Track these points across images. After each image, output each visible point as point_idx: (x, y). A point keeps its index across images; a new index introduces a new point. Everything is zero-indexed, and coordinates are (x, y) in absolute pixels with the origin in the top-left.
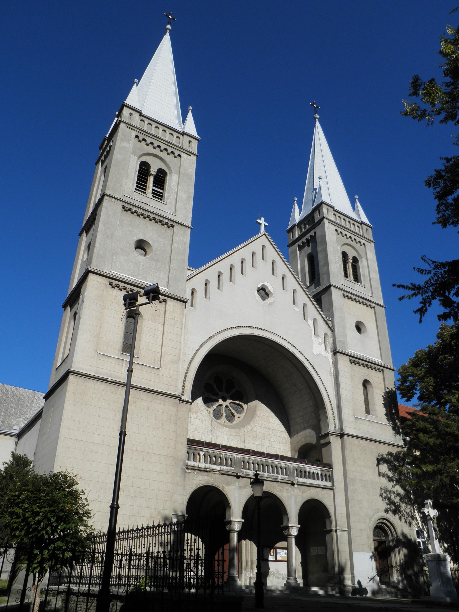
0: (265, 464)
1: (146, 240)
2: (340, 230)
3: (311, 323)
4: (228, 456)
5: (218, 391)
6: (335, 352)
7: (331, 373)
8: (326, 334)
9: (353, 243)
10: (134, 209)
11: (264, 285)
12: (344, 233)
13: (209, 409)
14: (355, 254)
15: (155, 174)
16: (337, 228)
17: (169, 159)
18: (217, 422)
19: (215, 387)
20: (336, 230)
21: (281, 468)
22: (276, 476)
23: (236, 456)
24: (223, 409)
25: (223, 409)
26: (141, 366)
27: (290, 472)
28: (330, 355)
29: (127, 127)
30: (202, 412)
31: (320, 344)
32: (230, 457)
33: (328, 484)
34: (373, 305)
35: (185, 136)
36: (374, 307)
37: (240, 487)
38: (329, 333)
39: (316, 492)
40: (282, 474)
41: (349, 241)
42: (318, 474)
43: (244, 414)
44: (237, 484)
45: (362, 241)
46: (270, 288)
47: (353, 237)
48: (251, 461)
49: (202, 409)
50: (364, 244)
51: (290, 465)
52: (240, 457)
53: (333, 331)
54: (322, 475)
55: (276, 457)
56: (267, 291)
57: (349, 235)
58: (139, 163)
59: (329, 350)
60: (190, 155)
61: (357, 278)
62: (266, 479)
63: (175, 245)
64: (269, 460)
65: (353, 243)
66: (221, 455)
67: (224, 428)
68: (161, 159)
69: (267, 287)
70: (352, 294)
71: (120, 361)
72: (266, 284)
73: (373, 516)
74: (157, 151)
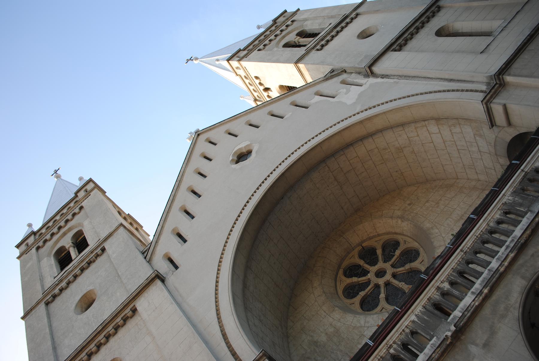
0: (469, 257)
1: (85, 292)
4: (402, 337)
5: (364, 278)
6: (369, 71)
7: (395, 82)
8: (343, 82)
10: (57, 291)
11: (235, 152)
13: (379, 308)
15: (71, 244)
18: (376, 313)
19: (355, 279)
20: (259, 50)
21: (499, 222)
22: (513, 240)
23: (413, 318)
24: (395, 282)
25: (395, 282)
27: (521, 205)
28: (372, 80)
30: (367, 325)
31: (348, 91)
32: (407, 331)
34: (353, 15)
37: (486, 345)
38: (344, 76)
40: (516, 223)
43: (421, 251)
44: (473, 349)
48: (446, 286)
49: (362, 322)
51: (504, 200)
52: (420, 308)
53: (345, 71)
55: (470, 224)
56: (244, 151)
59: (360, 80)
62: (502, 269)
64: (469, 242)
66: (392, 351)
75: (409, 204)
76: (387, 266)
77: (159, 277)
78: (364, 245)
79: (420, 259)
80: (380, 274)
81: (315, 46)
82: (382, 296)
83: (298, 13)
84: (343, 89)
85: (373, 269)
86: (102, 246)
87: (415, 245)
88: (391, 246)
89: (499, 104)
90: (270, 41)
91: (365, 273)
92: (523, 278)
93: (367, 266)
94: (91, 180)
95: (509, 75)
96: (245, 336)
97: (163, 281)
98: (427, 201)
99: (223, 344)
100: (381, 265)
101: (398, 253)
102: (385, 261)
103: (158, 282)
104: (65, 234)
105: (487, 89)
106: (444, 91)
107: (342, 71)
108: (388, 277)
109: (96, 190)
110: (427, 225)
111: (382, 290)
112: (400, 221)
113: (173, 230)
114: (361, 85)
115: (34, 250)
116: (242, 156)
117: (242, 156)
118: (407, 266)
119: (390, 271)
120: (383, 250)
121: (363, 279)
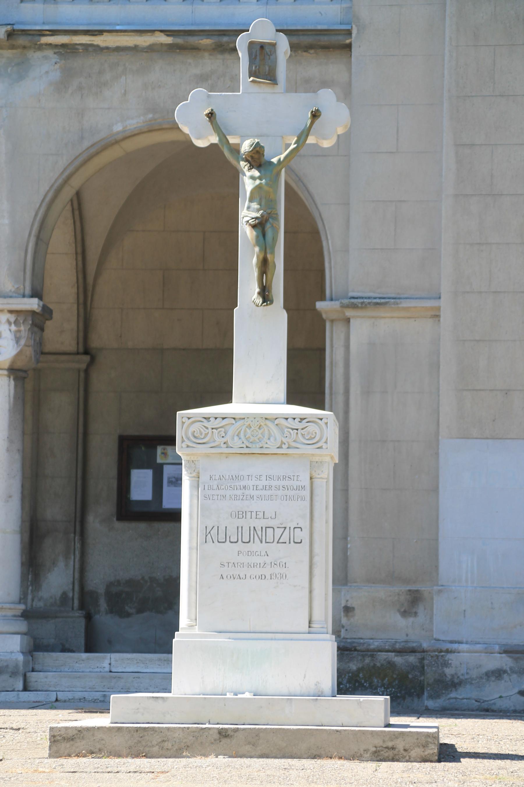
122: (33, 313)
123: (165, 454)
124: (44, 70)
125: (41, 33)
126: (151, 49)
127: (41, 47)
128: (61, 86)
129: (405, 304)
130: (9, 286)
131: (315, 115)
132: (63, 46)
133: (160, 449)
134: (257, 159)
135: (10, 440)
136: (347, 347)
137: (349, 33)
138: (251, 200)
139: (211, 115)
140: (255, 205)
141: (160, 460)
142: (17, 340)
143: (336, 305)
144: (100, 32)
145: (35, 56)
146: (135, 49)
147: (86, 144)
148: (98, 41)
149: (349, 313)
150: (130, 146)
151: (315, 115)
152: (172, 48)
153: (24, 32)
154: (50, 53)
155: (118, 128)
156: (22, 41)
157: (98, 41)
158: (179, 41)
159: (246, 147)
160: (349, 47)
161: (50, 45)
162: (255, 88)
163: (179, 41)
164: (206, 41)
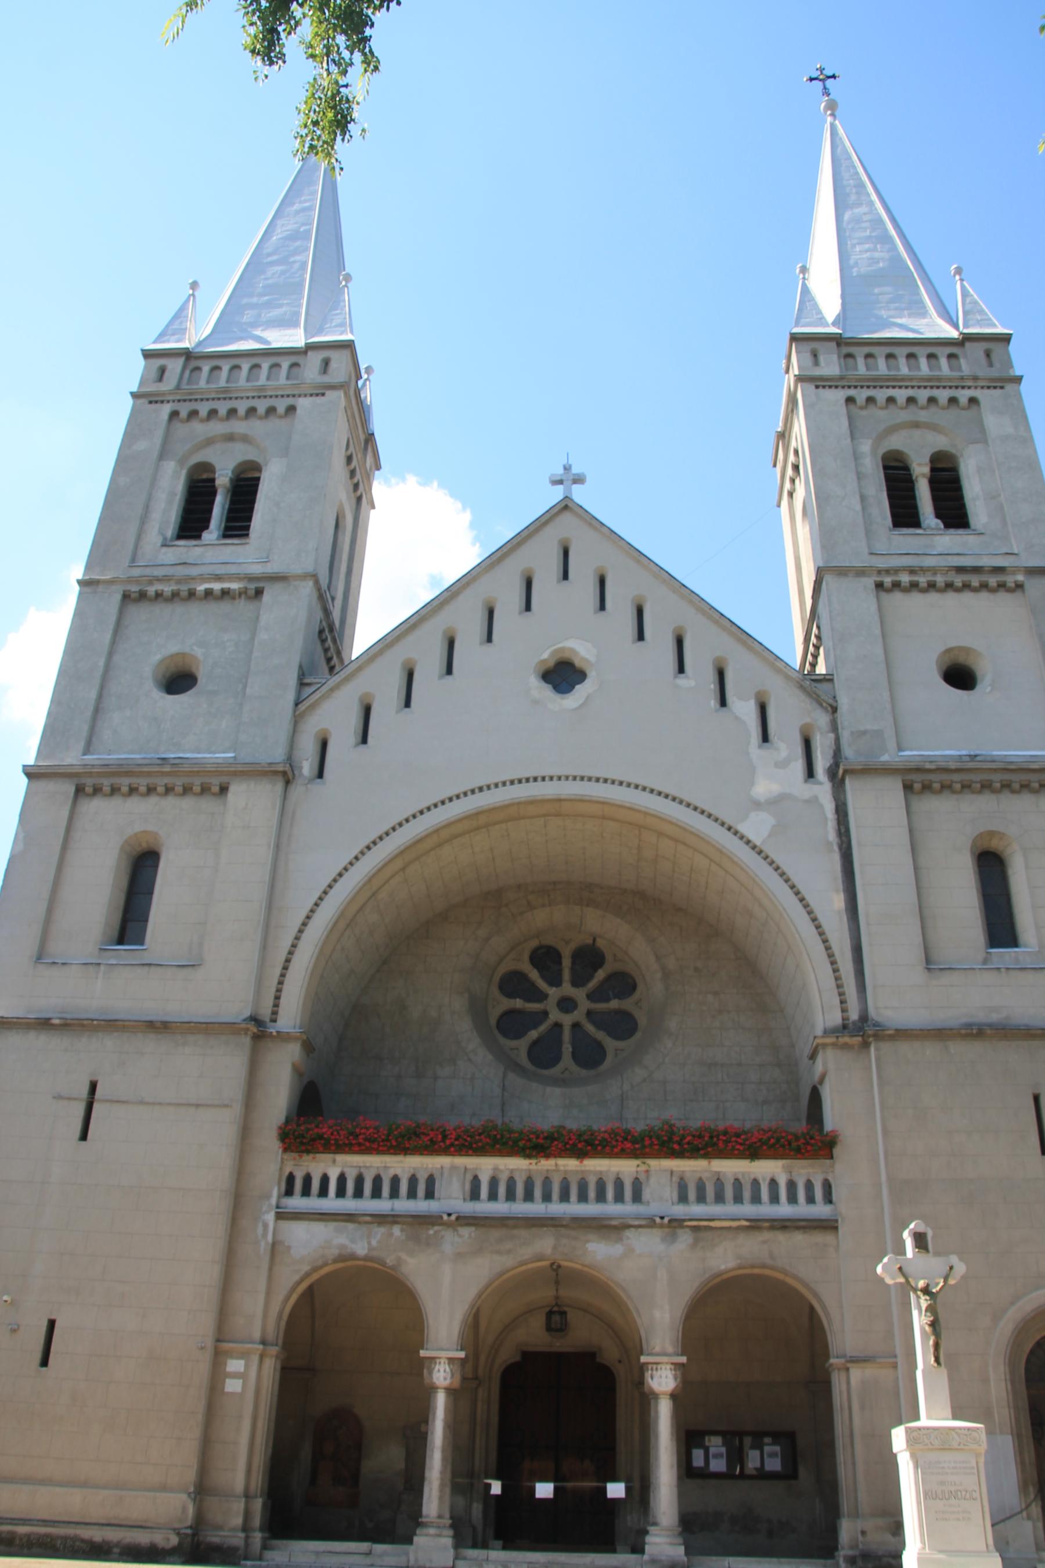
2: (861, 395)
3: (745, 709)
9: (923, 416)
11: (562, 649)
12: (881, 395)
14: (940, 442)
16: (852, 392)
17: (256, 428)
19: (534, 975)
26: (146, 968)
28: (823, 790)
29: (150, 402)
33: (820, 1210)
35: (309, 353)
36: (1019, 586)
38: (822, 719)
39: (765, 1242)
41: (905, 416)
42: (773, 1183)
43: (638, 1035)
45: (963, 396)
46: (583, 651)
47: (923, 395)
50: (973, 401)
54: (792, 1185)
57: (901, 395)
58: (183, 474)
60: (323, 394)
61: (954, 513)
63: (263, 636)
65: (923, 416)
67: (549, 1089)
68: (245, 439)
69: (573, 650)
70: (912, 571)
71: (91, 968)
72: (570, 644)
73: (1012, 1303)
74: (217, 428)
75: (696, 969)
76: (585, 1006)
77: (287, 776)
78: (600, 943)
79: (621, 1044)
80: (567, 1004)
81: (887, 571)
82: (534, 1034)
83: (1009, 387)
84: (787, 745)
85: (567, 989)
86: (261, 585)
87: (642, 1020)
88: (624, 983)
89: (825, 1064)
90: (891, 400)
91: (555, 981)
92: (555, 1248)
93: (566, 975)
94: (348, 346)
95: (877, 1049)
96: (304, 990)
97: (288, 782)
98: (716, 994)
99: (278, 971)
100: (579, 994)
101: (614, 1004)
102: (589, 997)
103: (279, 786)
104: (230, 438)
105: (854, 1023)
106: (831, 956)
107: (831, 706)
108: (567, 1020)
109: (341, 393)
110: (672, 1024)
111: (543, 1028)
112: (659, 975)
113: (367, 695)
114: (810, 773)
115: (166, 409)
116: (563, 675)
117: (563, 675)
118: (600, 1035)
119: (578, 1015)
120: (610, 977)
121: (542, 984)
122: (683, 1365)
123: (710, 1441)
124: (685, 1238)
125: (684, 1220)
126: (738, 1228)
127: (682, 1227)
128: (694, 1246)
129: (879, 1360)
130: (670, 1349)
131: (951, 1268)
132: (695, 1227)
133: (707, 1438)
134: (926, 1291)
135: (672, 1434)
136: (848, 1383)
137: (836, 1221)
138: (926, 1311)
139: (900, 1269)
140: (928, 1314)
141: (707, 1443)
142: (675, 1378)
143: (843, 1360)
144: (713, 1220)
145: (680, 1231)
146: (729, 1228)
147: (707, 1276)
148: (712, 1224)
149: (849, 1365)
150: (725, 1276)
151: (951, 1268)
152: (747, 1228)
153: (676, 1220)
154: (687, 1230)
155: (723, 1267)
156: (675, 1224)
157: (712, 1224)
158: (753, 1224)
159: (921, 1284)
160: (836, 1228)
161: (688, 1226)
162: (919, 1255)
163: (753, 1224)
164: (767, 1224)
